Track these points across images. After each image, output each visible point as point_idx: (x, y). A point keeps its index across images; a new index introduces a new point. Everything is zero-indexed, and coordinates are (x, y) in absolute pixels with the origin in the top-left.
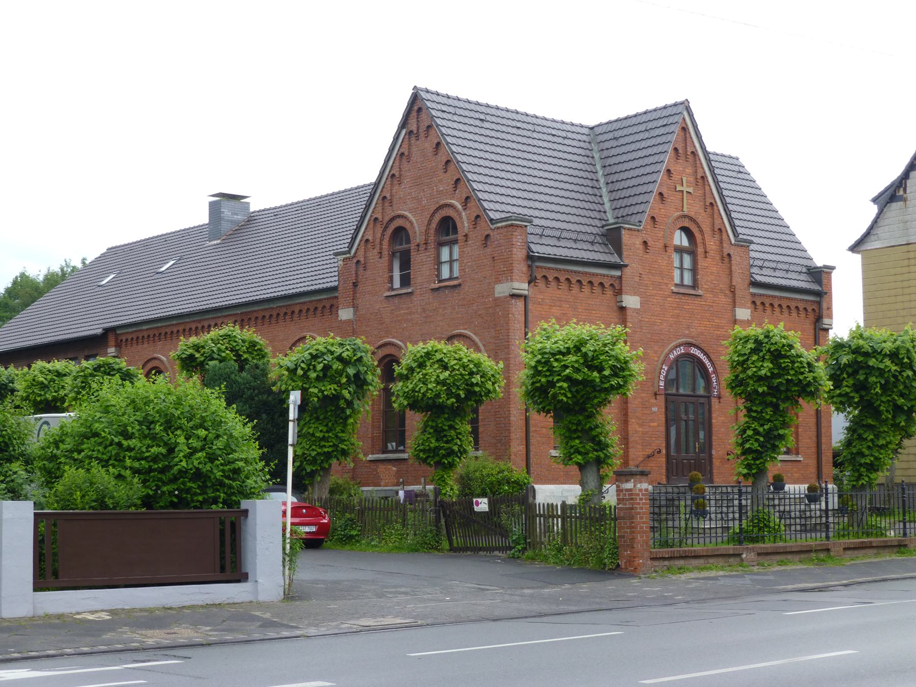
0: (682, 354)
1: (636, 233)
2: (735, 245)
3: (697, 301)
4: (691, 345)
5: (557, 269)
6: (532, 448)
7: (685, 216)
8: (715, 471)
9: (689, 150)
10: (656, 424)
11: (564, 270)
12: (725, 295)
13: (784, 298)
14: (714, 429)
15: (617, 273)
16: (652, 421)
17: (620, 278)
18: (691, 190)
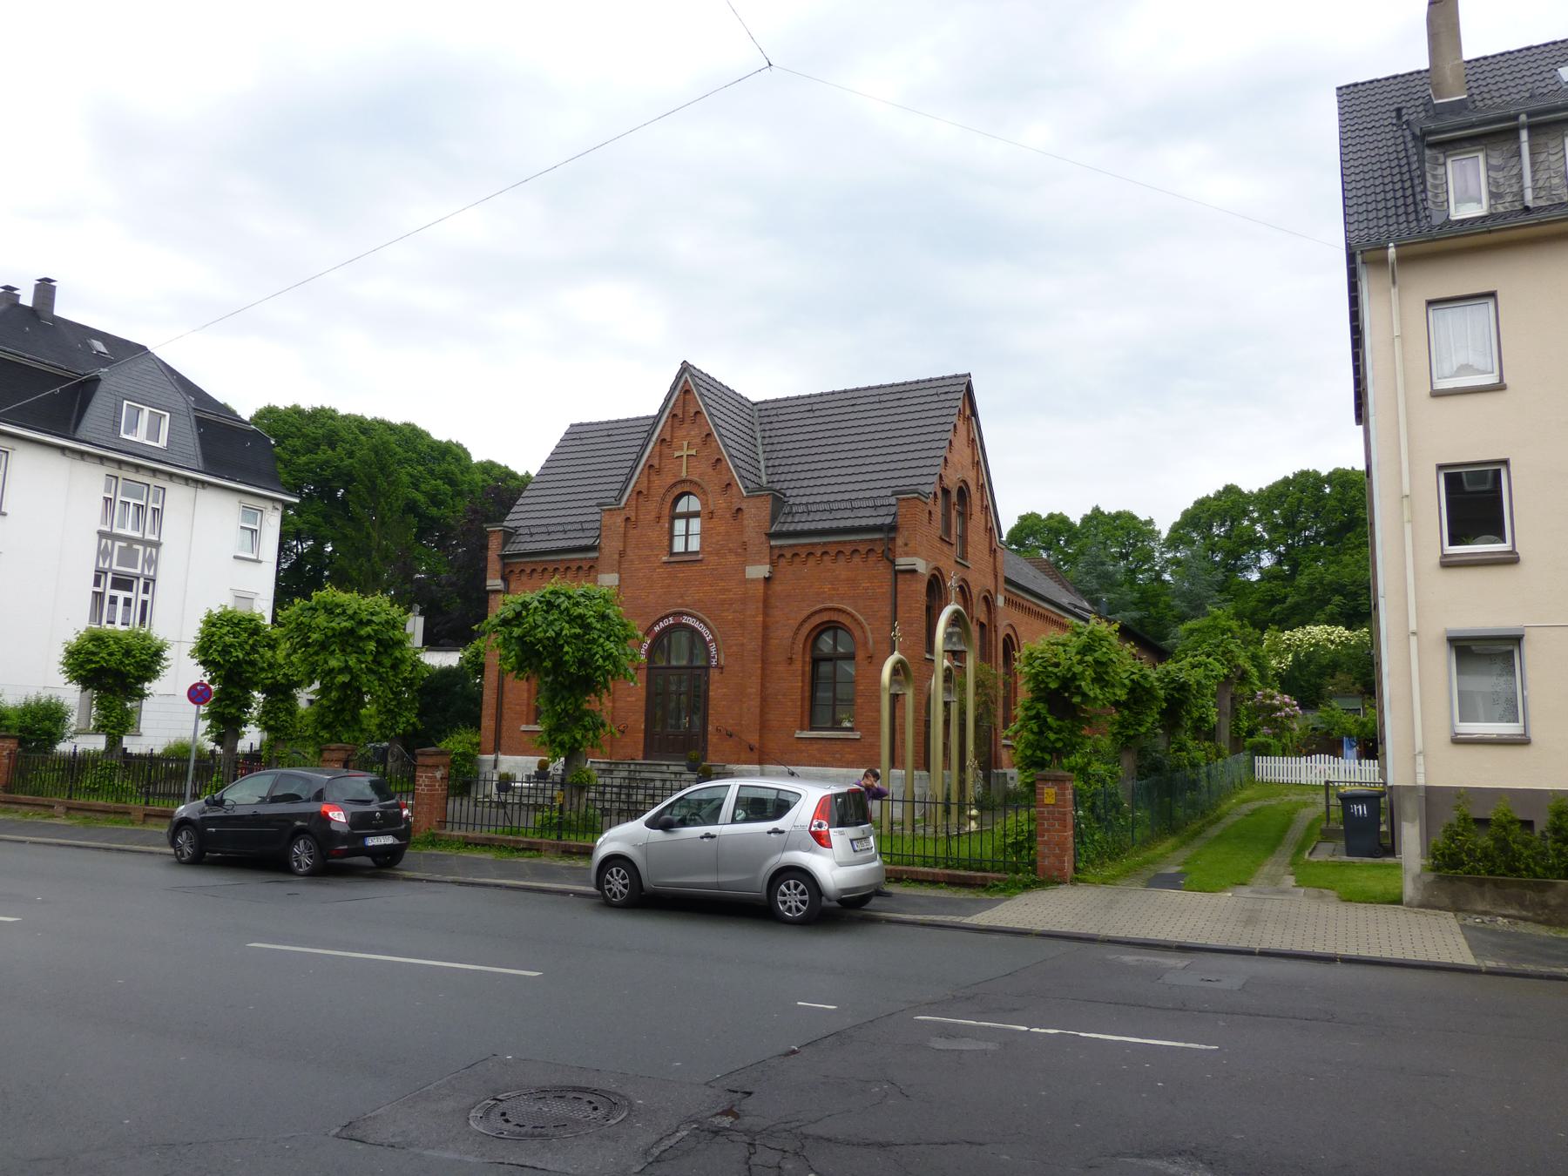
0: (670, 625)
1: (618, 511)
2: (748, 497)
3: (697, 567)
4: (682, 614)
5: (532, 562)
6: (504, 723)
7: (684, 481)
8: (710, 748)
9: (692, 411)
10: (633, 699)
11: (540, 561)
12: (737, 554)
13: (829, 543)
14: (712, 703)
15: (595, 555)
16: (629, 695)
17: (597, 558)
18: (693, 452)
